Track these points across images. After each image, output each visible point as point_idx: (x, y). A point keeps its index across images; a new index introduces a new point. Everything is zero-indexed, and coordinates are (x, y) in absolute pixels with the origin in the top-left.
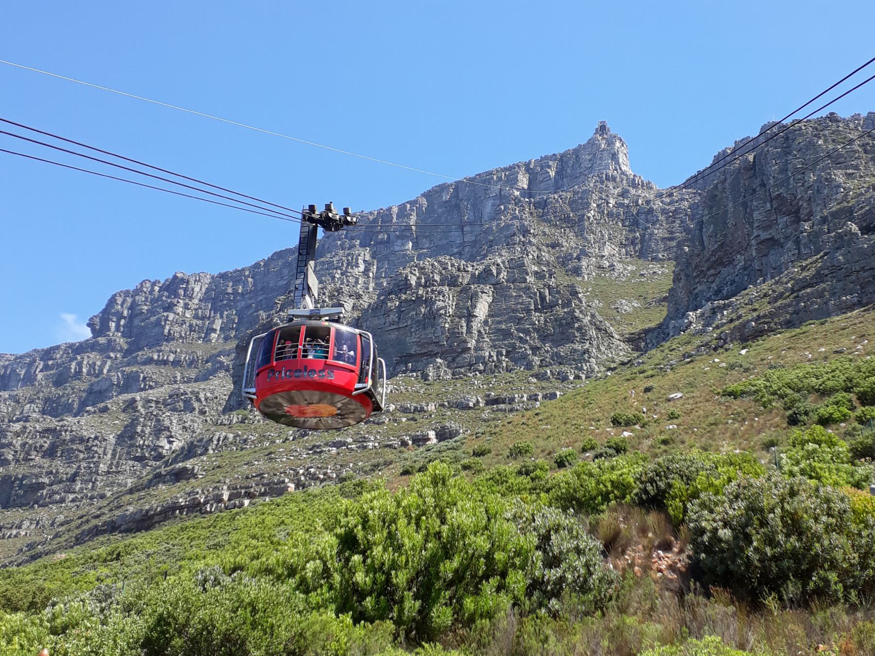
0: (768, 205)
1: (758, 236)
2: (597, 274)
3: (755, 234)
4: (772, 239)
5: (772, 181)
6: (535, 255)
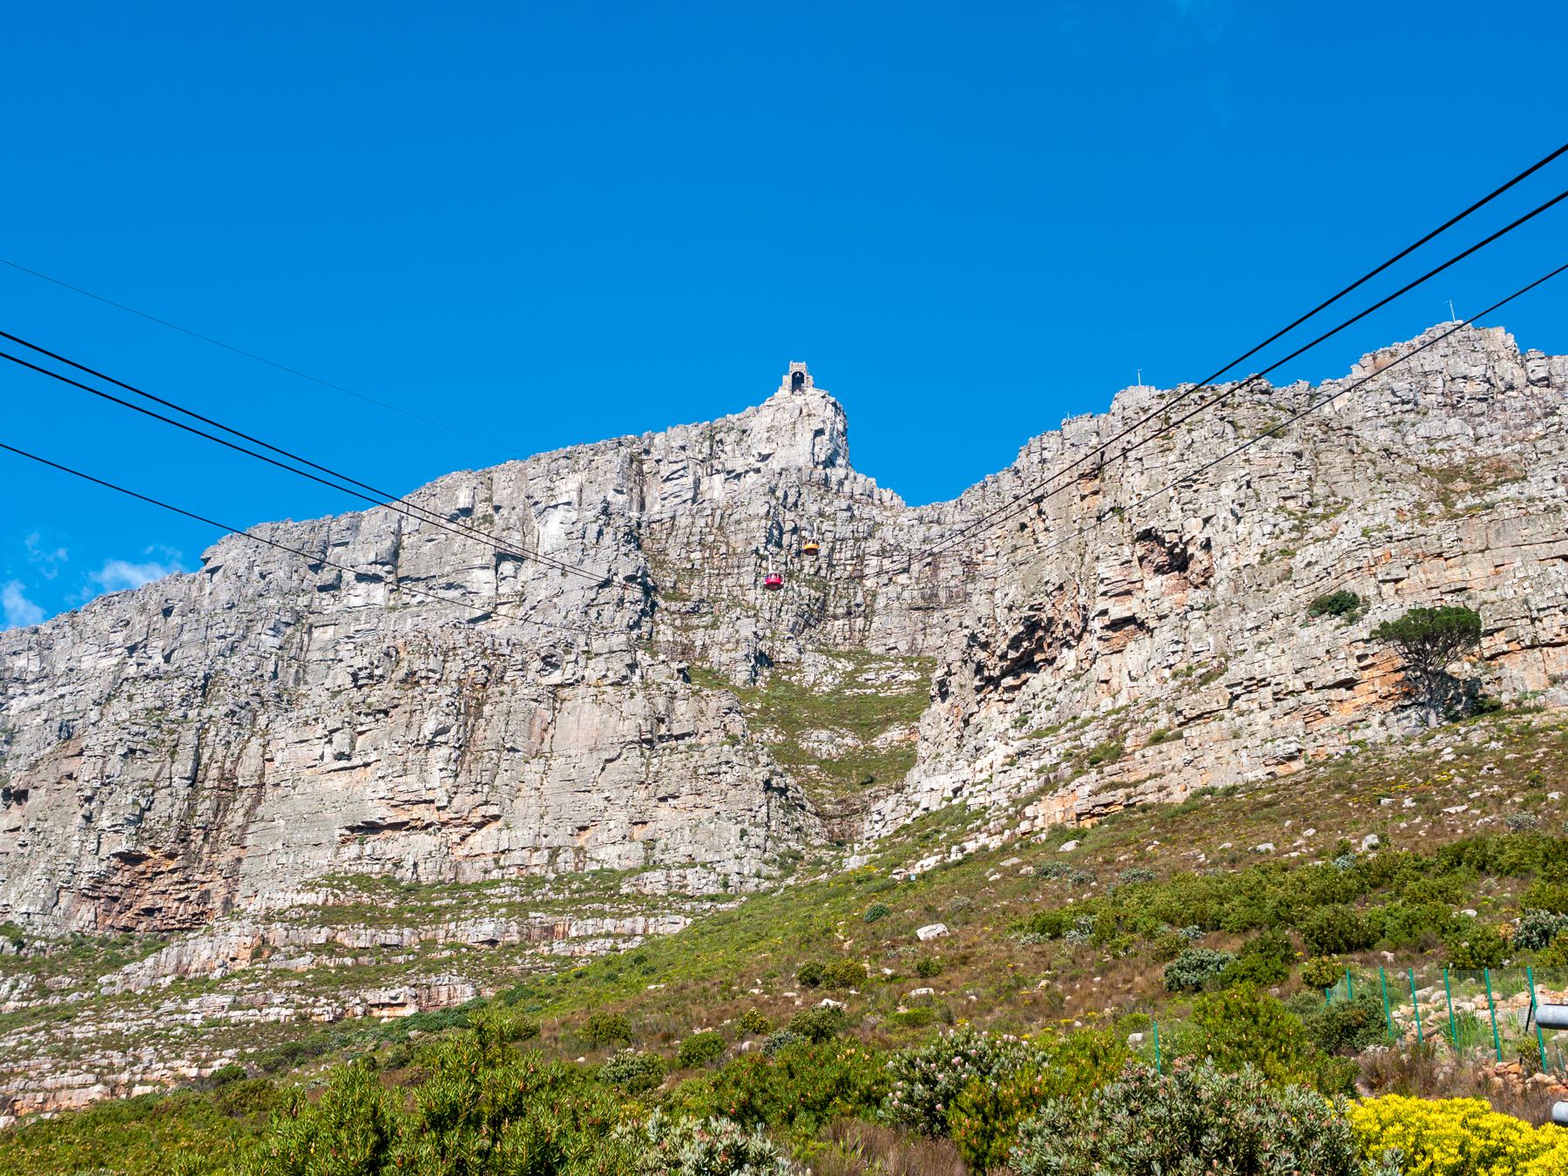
0: (1127, 551)
1: (1104, 613)
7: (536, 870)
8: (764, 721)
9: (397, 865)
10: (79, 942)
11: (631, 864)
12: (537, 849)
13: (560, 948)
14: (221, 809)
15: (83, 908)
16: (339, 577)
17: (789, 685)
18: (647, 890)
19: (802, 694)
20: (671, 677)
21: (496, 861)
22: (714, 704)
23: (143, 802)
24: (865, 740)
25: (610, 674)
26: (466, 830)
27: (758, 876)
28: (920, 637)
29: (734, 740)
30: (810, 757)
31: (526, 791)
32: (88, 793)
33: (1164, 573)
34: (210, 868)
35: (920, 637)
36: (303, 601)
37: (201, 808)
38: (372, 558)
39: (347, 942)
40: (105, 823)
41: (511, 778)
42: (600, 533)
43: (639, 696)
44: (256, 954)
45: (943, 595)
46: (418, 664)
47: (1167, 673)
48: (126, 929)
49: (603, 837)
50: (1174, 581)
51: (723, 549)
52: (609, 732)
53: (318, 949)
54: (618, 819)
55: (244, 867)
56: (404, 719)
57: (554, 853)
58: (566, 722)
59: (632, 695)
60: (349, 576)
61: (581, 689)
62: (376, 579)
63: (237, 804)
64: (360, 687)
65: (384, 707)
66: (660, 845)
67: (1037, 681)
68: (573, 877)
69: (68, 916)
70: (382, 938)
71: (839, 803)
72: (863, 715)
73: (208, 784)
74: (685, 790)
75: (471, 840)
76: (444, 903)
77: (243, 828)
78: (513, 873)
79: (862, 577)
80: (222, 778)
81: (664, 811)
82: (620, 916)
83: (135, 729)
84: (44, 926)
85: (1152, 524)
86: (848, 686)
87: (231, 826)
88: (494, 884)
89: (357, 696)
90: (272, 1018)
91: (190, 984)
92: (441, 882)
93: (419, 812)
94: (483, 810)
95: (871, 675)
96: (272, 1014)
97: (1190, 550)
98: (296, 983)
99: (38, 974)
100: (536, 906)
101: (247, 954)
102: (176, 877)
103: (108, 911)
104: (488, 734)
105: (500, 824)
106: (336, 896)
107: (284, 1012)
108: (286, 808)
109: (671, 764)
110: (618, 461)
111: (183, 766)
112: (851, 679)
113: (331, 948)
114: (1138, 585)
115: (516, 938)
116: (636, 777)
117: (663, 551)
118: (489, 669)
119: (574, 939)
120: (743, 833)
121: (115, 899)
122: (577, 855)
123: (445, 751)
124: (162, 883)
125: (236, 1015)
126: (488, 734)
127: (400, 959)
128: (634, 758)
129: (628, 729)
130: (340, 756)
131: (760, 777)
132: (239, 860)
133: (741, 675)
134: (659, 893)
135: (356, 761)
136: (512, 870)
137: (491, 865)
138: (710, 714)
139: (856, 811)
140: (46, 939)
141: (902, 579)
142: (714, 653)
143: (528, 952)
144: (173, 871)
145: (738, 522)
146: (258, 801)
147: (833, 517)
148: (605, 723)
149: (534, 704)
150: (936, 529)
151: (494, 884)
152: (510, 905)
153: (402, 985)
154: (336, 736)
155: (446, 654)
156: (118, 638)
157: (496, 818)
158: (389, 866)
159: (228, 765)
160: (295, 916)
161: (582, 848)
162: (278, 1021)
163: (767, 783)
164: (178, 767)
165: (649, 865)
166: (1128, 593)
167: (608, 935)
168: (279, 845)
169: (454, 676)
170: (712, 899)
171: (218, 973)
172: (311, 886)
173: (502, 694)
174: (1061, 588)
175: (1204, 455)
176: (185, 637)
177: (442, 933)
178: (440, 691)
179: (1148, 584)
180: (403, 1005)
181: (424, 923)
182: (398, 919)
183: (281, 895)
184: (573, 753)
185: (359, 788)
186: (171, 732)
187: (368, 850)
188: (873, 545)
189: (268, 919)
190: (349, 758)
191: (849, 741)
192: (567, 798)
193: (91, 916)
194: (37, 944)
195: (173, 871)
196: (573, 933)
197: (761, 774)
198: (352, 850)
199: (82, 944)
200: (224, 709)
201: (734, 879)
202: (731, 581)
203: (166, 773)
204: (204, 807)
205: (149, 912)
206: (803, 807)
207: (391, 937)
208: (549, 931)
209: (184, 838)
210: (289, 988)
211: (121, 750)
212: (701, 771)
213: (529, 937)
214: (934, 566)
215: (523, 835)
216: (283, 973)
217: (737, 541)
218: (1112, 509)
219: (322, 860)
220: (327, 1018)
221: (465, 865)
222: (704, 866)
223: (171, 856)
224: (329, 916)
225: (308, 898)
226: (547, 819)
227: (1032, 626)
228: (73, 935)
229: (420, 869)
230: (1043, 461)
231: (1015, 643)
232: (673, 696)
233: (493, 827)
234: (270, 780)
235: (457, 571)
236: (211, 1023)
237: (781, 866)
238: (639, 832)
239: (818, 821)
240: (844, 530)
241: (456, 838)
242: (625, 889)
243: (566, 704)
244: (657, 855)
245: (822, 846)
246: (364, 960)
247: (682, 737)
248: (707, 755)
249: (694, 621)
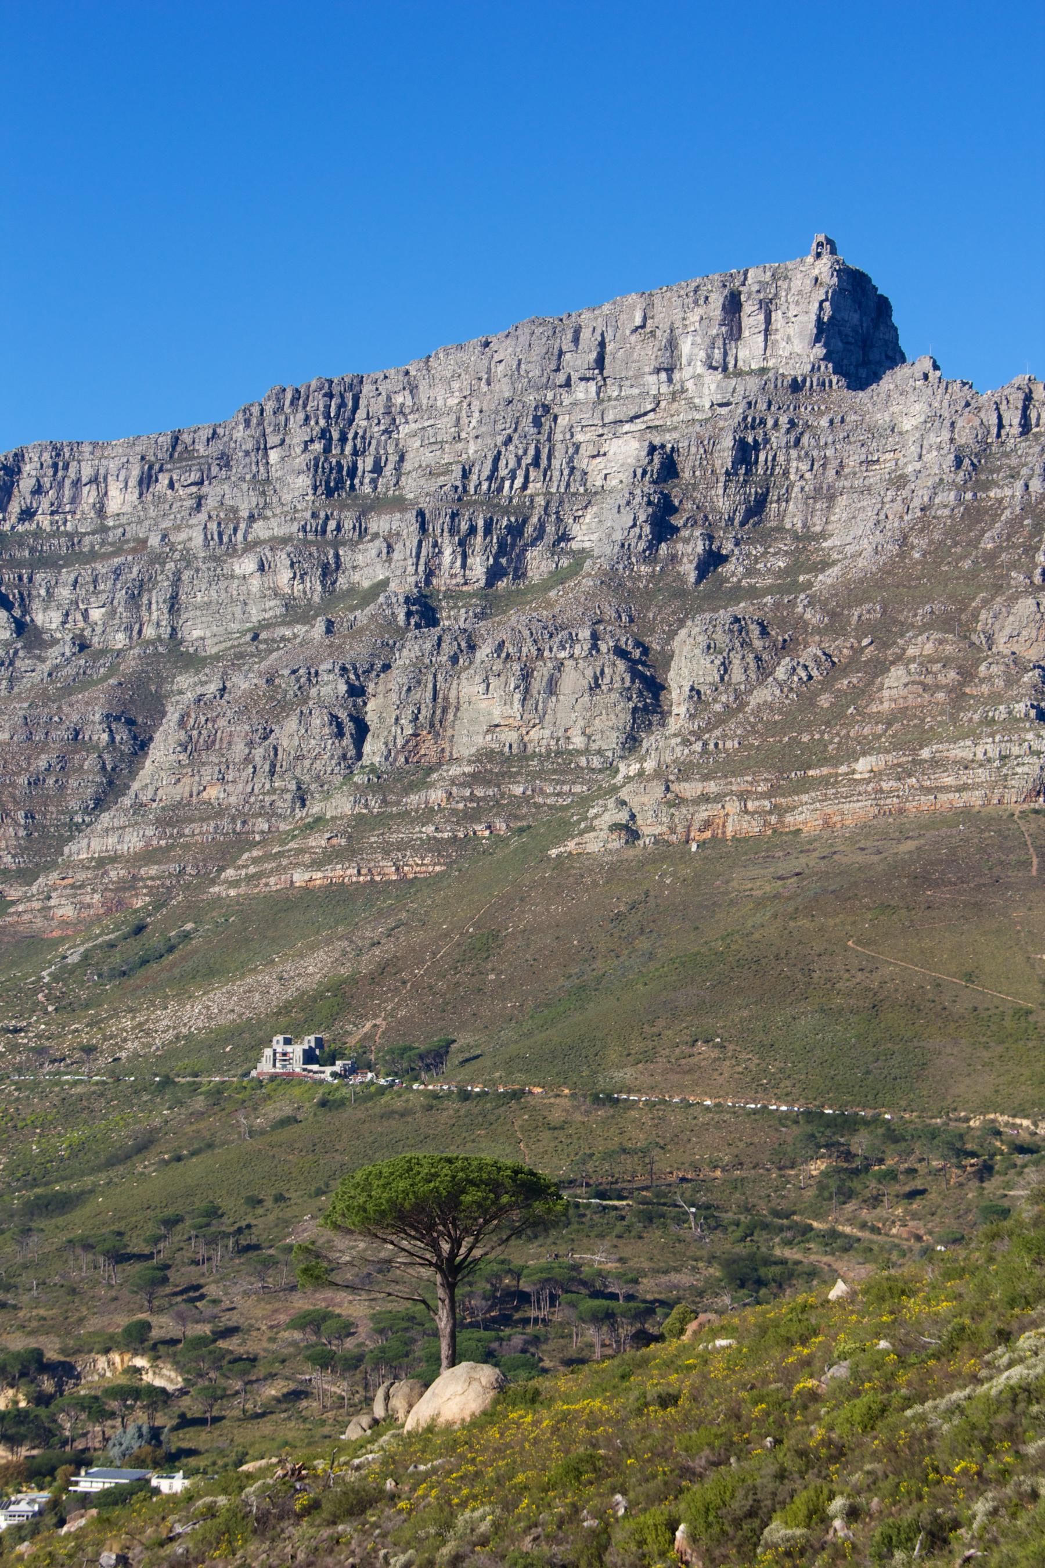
16: (569, 378)
60: (574, 377)
69: (395, 760)
93: (511, 721)
111: (429, 694)
124: (427, 744)
198: (489, 737)
215: (547, 733)
217: (718, 463)
236: (429, 838)
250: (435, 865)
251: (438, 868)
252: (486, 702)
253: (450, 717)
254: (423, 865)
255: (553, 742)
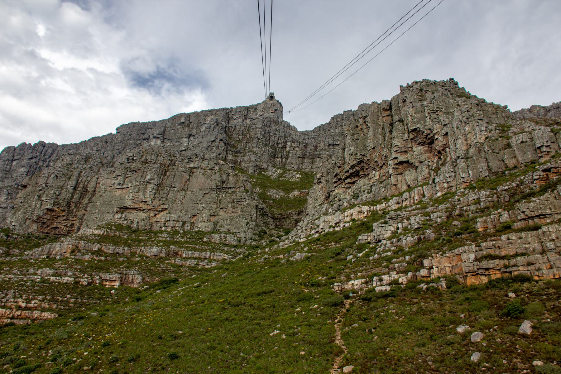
0: (406, 136)
1: (396, 158)
2: (259, 172)
3: (394, 156)
4: (407, 162)
5: (410, 118)
6: (224, 155)
7: (177, 228)
8: (256, 185)
9: (132, 222)
10: (29, 236)
11: (209, 230)
12: (178, 221)
13: (178, 261)
14: (81, 198)
15: (34, 225)
17: (264, 175)
18: (213, 240)
19: (268, 178)
20: (229, 169)
21: (165, 224)
22: (241, 179)
23: (57, 193)
24: (287, 194)
25: (209, 166)
26: (156, 212)
27: (251, 239)
28: (301, 165)
29: (247, 191)
30: (270, 198)
31: (177, 201)
32: (41, 188)
33: (422, 145)
34: (75, 216)
35: (301, 165)
36: (139, 142)
37: (75, 197)
38: (158, 132)
39: (105, 250)
40: (44, 198)
41: (173, 197)
42: (214, 127)
43: (218, 174)
44: (73, 252)
45: (308, 154)
46: (149, 157)
47: (446, 185)
48: (47, 233)
49: (200, 219)
50: (426, 149)
51: (248, 136)
52: (207, 185)
53: (93, 252)
54: (206, 214)
55: (85, 217)
56: (141, 174)
57: (184, 223)
58: (193, 180)
59: (215, 173)
60: (151, 136)
61: (199, 170)
62: (158, 138)
63: (87, 196)
64: (129, 163)
65: (135, 169)
66: (219, 224)
67: (361, 182)
68: (190, 232)
69: (28, 227)
70: (117, 250)
71: (280, 214)
72: (287, 187)
73: (79, 189)
74: (230, 206)
75: (157, 216)
76: (143, 238)
77: (87, 204)
78: (169, 229)
79: (286, 147)
80: (83, 188)
81: (222, 213)
82: (201, 250)
83: (59, 169)
84: (19, 230)
85: (418, 126)
86: (281, 177)
87: (84, 203)
88: (161, 232)
89: (127, 165)
90: (65, 281)
91: (50, 261)
92: (145, 229)
94: (162, 206)
95: (287, 175)
96: (66, 279)
97: (436, 137)
98: (79, 267)
99: (8, 248)
100: (173, 243)
101: (70, 251)
102: (64, 218)
103: (42, 227)
104: (167, 182)
105: (167, 211)
106: (107, 232)
107: (70, 279)
108: (101, 199)
109: (226, 197)
110: (223, 113)
111: (73, 182)
112: (281, 175)
113: (99, 252)
114: (410, 149)
115: (164, 255)
116: (214, 200)
117: (232, 135)
118: (172, 160)
119: (184, 258)
120: (248, 223)
121: (45, 223)
122: (191, 225)
123: (152, 186)
124: (60, 220)
125: (53, 278)
126: (167, 181)
127: (121, 259)
128: (214, 194)
129: (213, 185)
130: (119, 184)
131: (255, 204)
132: (84, 215)
133: (251, 171)
134: (217, 242)
135: (124, 186)
136: (169, 228)
137: (163, 225)
138: (240, 182)
139: (284, 218)
140: (17, 235)
141: (297, 149)
142: (243, 164)
143: (166, 262)
144: (63, 216)
145: (253, 129)
146: (93, 196)
147: (279, 130)
148: (205, 181)
149: (183, 173)
150: (306, 136)
151: (161, 232)
152: (165, 241)
153: (116, 272)
154: (119, 178)
155: (158, 155)
156: (95, 148)
157: (166, 209)
158: (129, 222)
159: (86, 183)
160: (91, 238)
161: (193, 222)
162: (66, 283)
163: (257, 206)
164: (70, 183)
165: (214, 231)
166: (406, 152)
167: (196, 258)
168: (97, 211)
169: (159, 162)
170: (235, 246)
171: (58, 257)
172: (100, 227)
173: (173, 169)
174: (374, 148)
175: (440, 102)
176: (108, 148)
177: (139, 250)
178: (154, 166)
179: (414, 149)
180: (115, 281)
181: (134, 246)
182: (126, 244)
183: (88, 230)
184: (194, 190)
185: (124, 195)
186: (72, 171)
187: (124, 215)
188: (290, 139)
189: (81, 239)
190: (122, 185)
191: (282, 194)
192: (190, 205)
193: (36, 228)
194: (14, 236)
195: (63, 216)
196: (184, 255)
197: (255, 203)
198: (119, 215)
199: (30, 237)
200: (89, 166)
201: (243, 239)
202: (250, 145)
203: (66, 184)
204: (76, 196)
205: (55, 228)
206: (267, 215)
207: (120, 250)
208: (176, 254)
209: (68, 205)
210: (76, 269)
211: (53, 176)
212: (235, 200)
213: (169, 255)
214: (306, 146)
215: (174, 216)
216: (77, 261)
217: (252, 134)
218: (399, 121)
219: (109, 217)
220: (85, 283)
221: (154, 224)
222: (233, 234)
223: (63, 211)
224: (102, 239)
225: (97, 232)
226: (183, 212)
227: (360, 163)
228: (28, 234)
229: (139, 224)
230: (337, 121)
231: (353, 167)
232: (228, 175)
233: (164, 213)
234: (98, 190)
235: (179, 138)
236: (43, 281)
237: (259, 236)
238: (213, 219)
239: (272, 220)
240: (283, 135)
241: (152, 215)
242: (205, 240)
243: (194, 174)
244: (218, 228)
245: (273, 229)
246: (109, 258)
247: (231, 188)
248: (238, 195)
249: (238, 154)
250: (43, 310)
251: (46, 315)
252: (120, 191)
253: (86, 201)
254: (26, 308)
255: (179, 225)
